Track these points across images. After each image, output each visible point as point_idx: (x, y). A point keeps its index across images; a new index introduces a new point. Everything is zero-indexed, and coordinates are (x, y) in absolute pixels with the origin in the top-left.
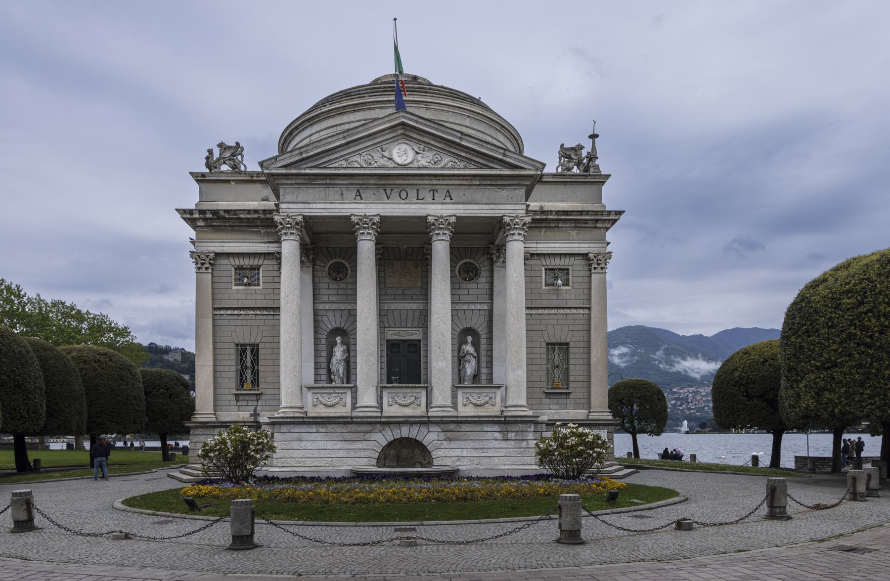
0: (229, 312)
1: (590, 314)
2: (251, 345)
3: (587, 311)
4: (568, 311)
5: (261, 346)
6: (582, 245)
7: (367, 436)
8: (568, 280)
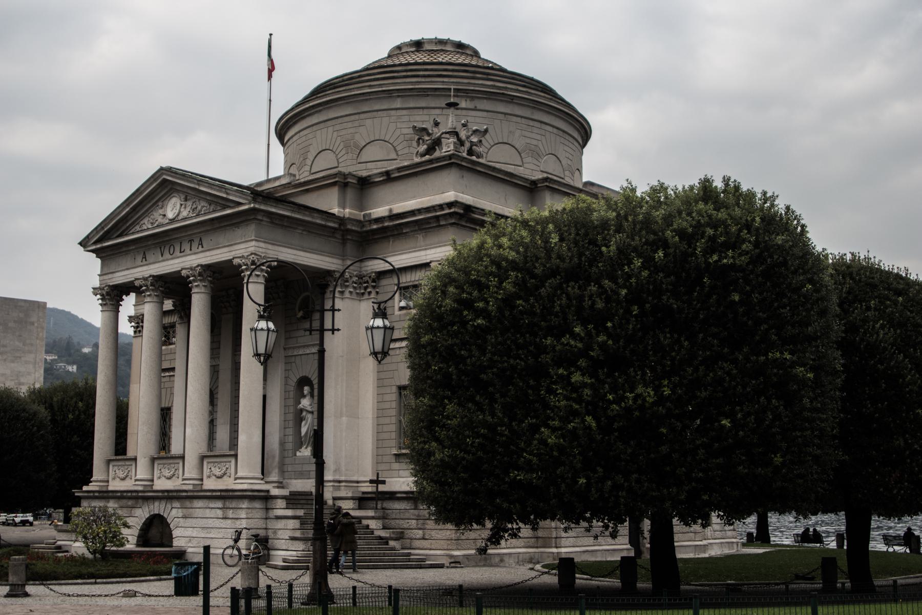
6: (428, 252)
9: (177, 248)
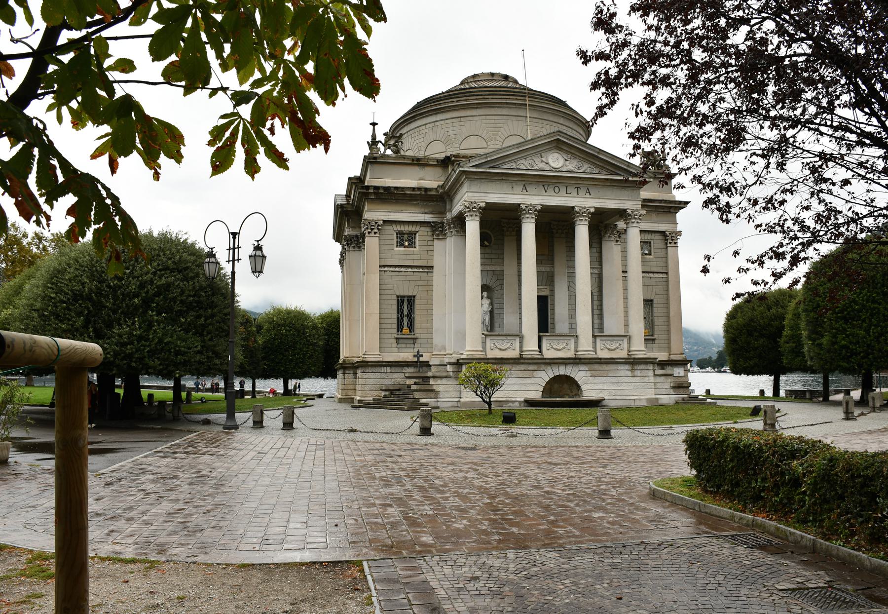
0: (392, 269)
1: (667, 278)
2: (408, 297)
3: (665, 276)
4: (652, 275)
5: (417, 298)
7: (535, 374)
8: (650, 251)
9: (563, 190)
